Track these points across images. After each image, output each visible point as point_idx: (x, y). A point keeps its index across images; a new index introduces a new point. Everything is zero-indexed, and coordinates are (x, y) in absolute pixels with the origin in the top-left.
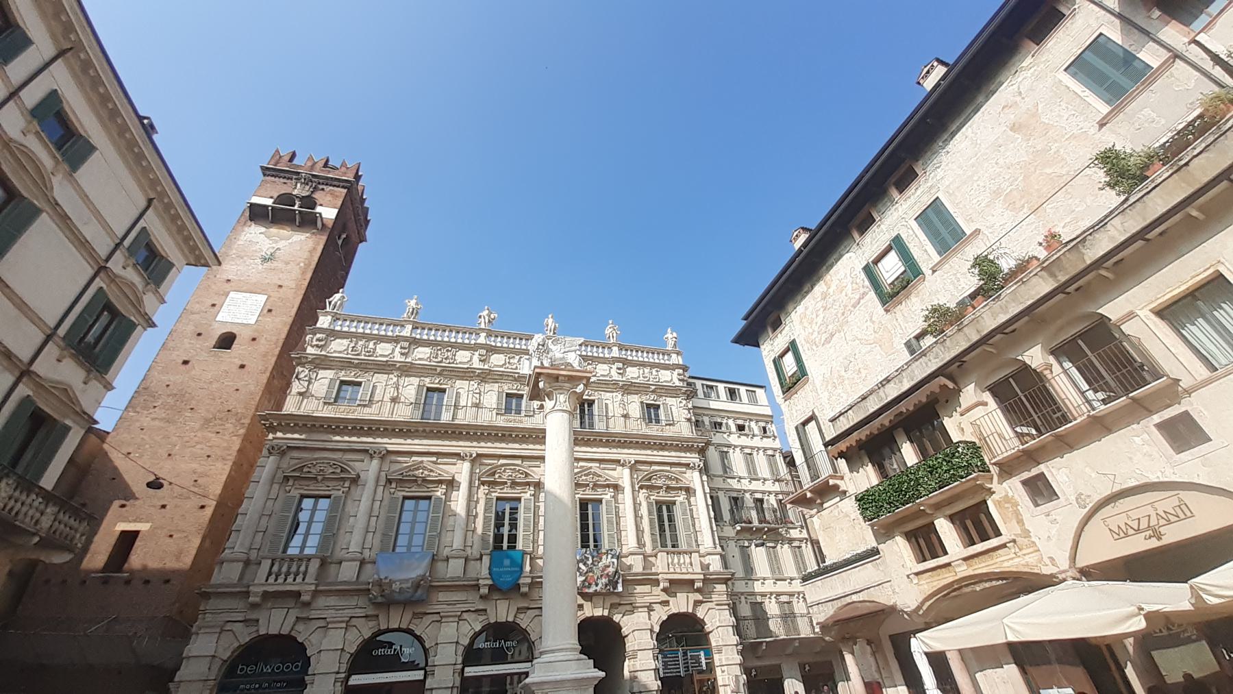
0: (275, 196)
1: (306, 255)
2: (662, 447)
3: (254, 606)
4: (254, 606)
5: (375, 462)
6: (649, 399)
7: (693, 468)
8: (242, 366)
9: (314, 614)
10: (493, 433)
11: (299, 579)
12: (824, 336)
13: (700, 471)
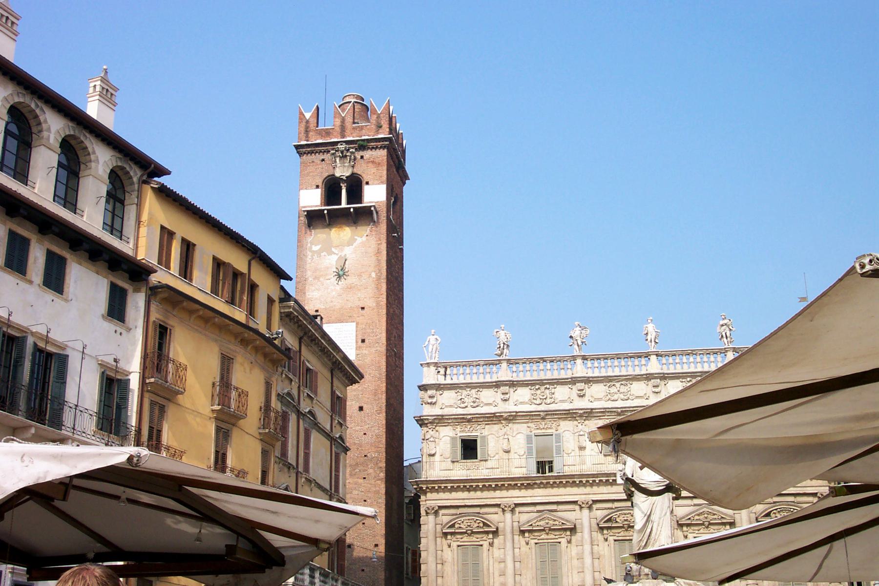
0: (319, 181)
1: (374, 258)
8: (361, 409)
10: (604, 479)
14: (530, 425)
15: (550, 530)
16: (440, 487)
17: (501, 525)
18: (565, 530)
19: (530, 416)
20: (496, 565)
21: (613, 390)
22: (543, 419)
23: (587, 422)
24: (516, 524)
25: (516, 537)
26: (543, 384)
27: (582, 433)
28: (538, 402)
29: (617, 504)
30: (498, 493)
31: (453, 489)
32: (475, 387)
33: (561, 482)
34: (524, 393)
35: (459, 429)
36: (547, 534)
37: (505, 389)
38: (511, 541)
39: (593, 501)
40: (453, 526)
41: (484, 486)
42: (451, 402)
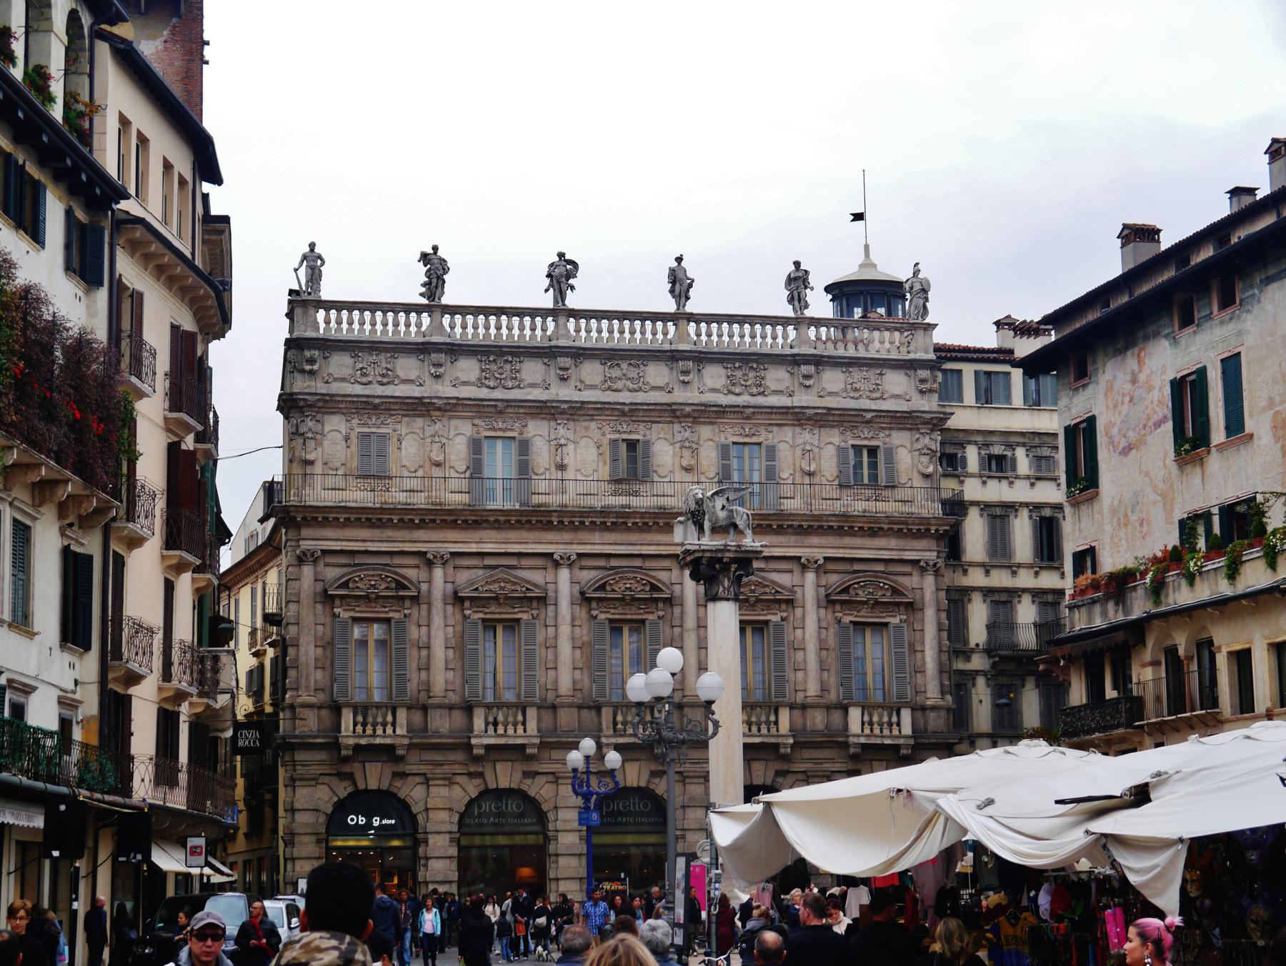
2: (873, 532)
3: (346, 760)
4: (346, 760)
5: (438, 573)
6: (866, 437)
7: (923, 570)
9: (408, 769)
10: (598, 520)
11: (389, 730)
12: (1123, 443)
13: (937, 573)
14: (476, 421)
15: (507, 598)
16: (325, 519)
17: (424, 587)
18: (531, 599)
19: (479, 408)
20: (415, 652)
21: (616, 373)
22: (501, 412)
23: (571, 425)
24: (450, 587)
25: (450, 608)
26: (502, 354)
27: (563, 441)
28: (492, 384)
29: (614, 563)
30: (420, 534)
31: (348, 523)
32: (386, 350)
33: (529, 522)
34: (468, 368)
35: (355, 421)
36: (500, 604)
37: (442, 357)
38: (442, 614)
39: (578, 554)
40: (345, 585)
41: (401, 520)
42: (346, 372)
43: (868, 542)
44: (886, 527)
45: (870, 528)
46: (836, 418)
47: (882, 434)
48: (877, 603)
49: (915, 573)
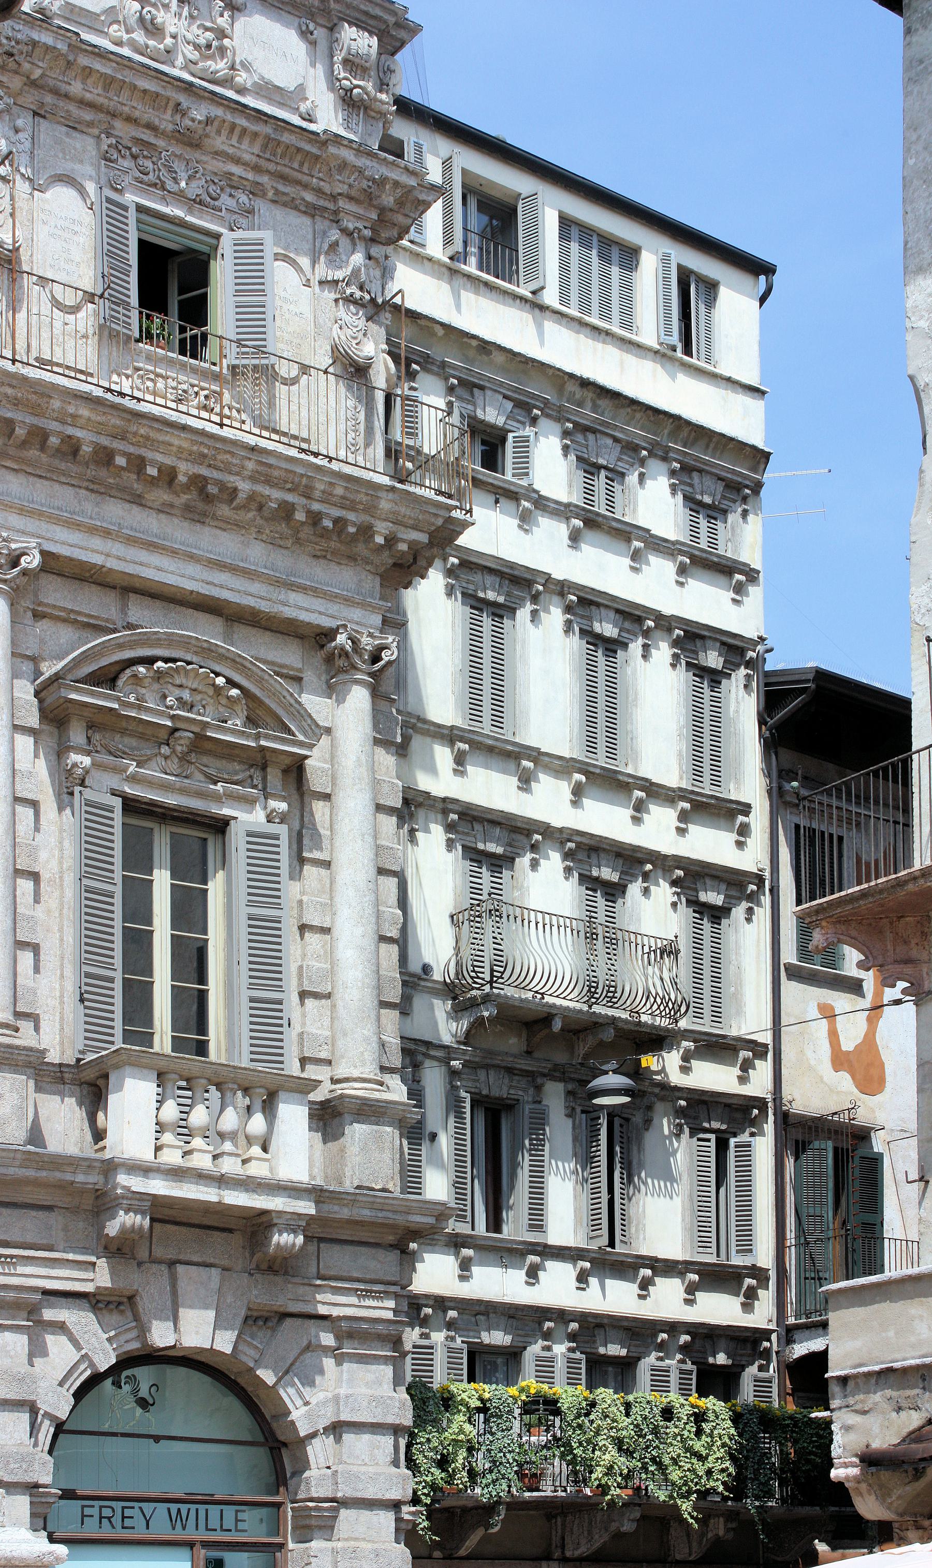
43: (179, 532)
44: (244, 487)
45: (198, 483)
46: (95, 93)
47: (226, 201)
48: (202, 744)
49: (309, 676)
